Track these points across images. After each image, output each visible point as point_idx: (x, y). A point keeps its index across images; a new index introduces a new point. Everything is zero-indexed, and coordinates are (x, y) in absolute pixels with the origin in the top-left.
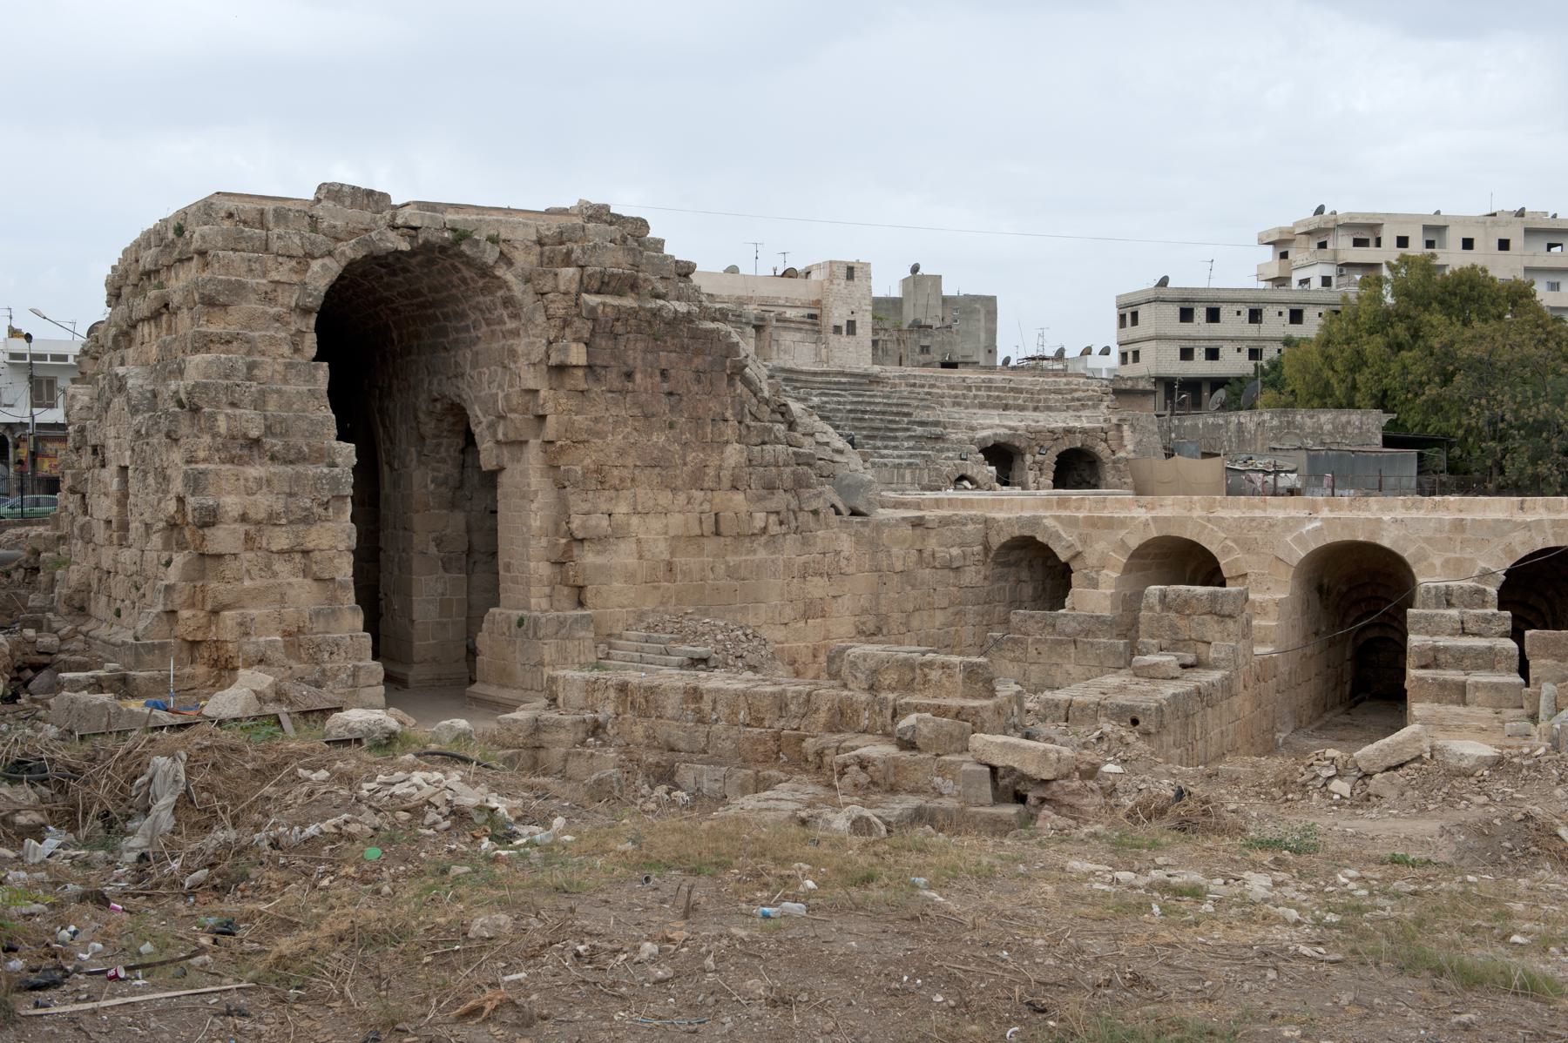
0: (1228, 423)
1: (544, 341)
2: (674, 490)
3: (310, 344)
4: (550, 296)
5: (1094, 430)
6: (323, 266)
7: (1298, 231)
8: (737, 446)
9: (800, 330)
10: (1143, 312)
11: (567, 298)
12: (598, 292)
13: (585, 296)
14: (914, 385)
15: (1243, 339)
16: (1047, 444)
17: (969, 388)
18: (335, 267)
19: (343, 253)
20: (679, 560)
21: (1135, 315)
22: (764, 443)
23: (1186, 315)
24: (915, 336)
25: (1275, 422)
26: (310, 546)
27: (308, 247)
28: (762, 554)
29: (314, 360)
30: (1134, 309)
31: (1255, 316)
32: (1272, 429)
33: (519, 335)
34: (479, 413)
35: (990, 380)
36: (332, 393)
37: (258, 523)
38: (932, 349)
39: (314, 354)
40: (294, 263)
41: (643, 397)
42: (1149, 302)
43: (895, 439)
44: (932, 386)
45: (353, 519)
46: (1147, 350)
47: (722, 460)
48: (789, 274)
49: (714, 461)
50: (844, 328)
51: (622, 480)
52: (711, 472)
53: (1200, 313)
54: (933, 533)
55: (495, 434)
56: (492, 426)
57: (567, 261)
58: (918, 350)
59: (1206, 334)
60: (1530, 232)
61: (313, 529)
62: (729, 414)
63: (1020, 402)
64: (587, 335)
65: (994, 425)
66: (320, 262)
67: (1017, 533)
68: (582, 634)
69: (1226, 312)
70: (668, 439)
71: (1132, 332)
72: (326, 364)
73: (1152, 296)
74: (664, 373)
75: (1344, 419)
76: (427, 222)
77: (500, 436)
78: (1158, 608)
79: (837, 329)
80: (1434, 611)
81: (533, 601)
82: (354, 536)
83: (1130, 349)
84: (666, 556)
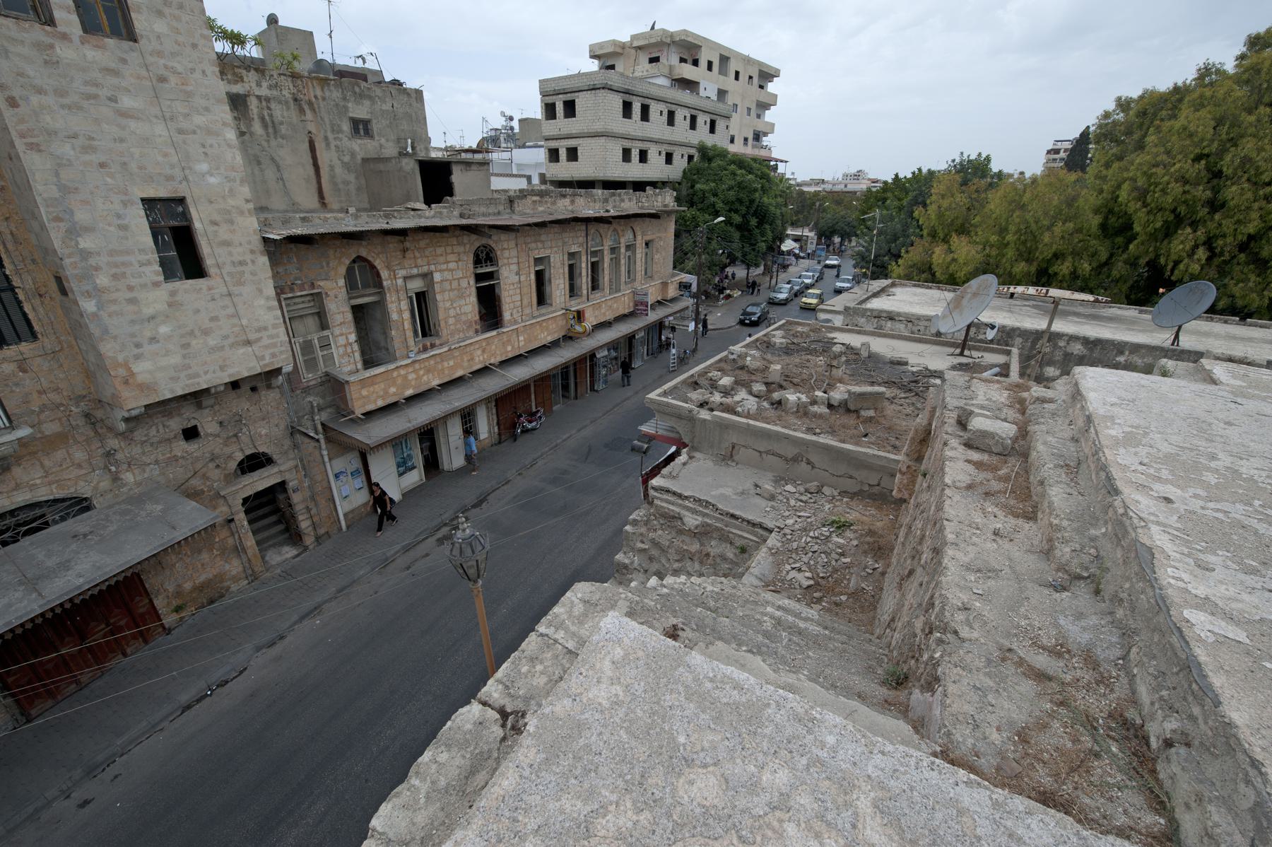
7: (636, 44)
10: (581, 102)
23: (627, 109)
24: (336, 94)
38: (375, 127)
42: (594, 89)
46: (584, 147)
58: (346, 127)
59: (639, 134)
71: (562, 124)
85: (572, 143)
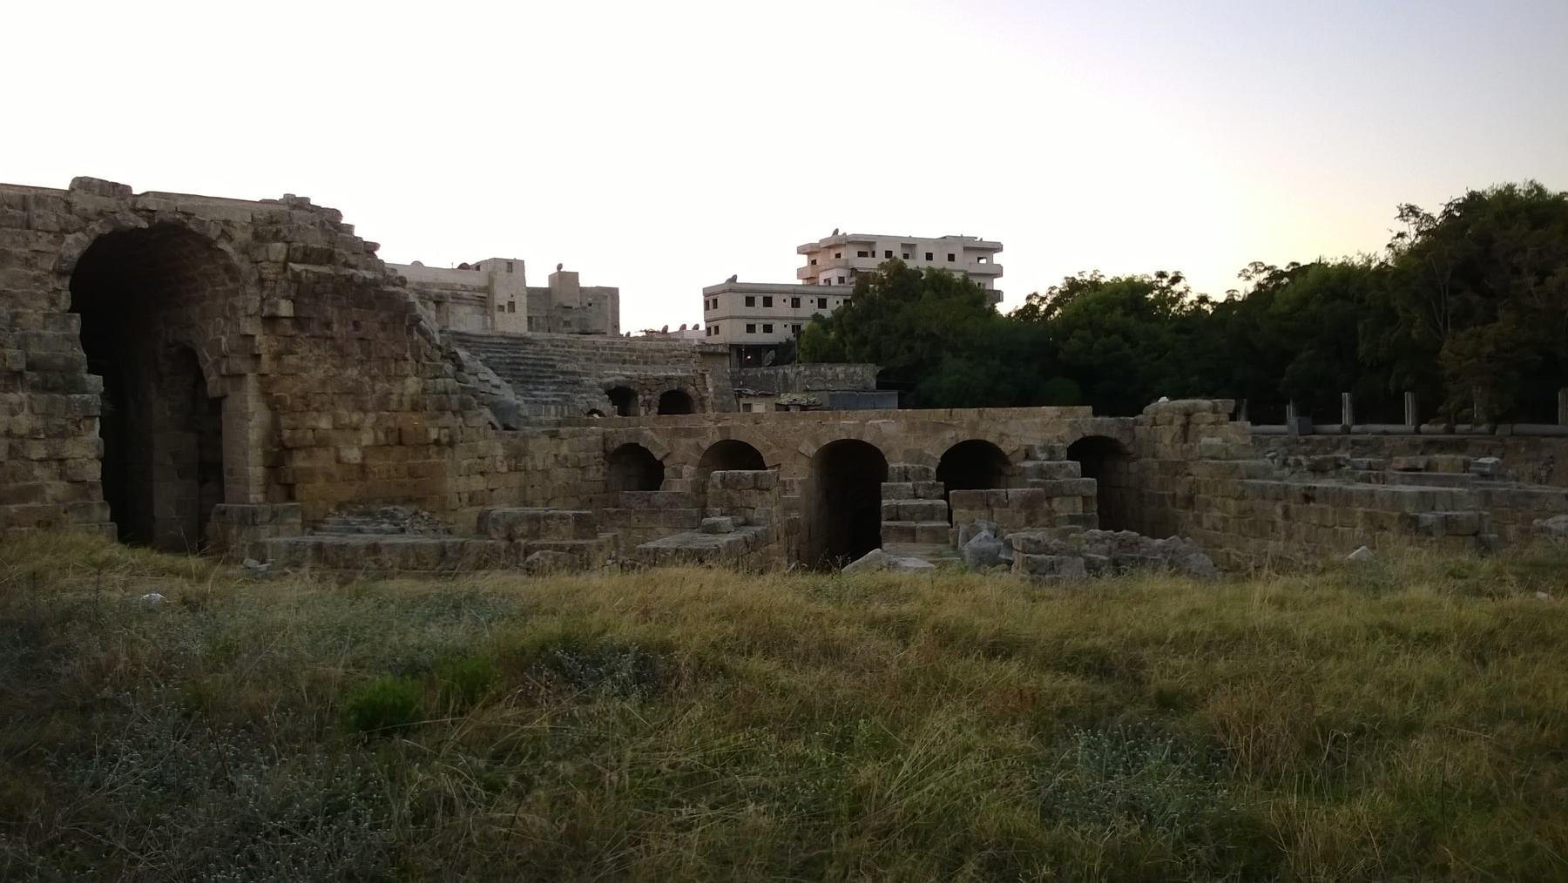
0: (777, 373)
1: (259, 298)
2: (365, 412)
3: (65, 300)
4: (264, 264)
5: (687, 377)
6: (77, 240)
7: (822, 246)
8: (415, 379)
9: (470, 304)
10: (720, 298)
11: (276, 266)
12: (302, 262)
13: (291, 264)
14: (557, 346)
15: (787, 318)
16: (653, 388)
17: (598, 349)
18: (85, 239)
19: (93, 230)
20: (369, 462)
21: (715, 301)
22: (437, 377)
23: (750, 302)
25: (807, 373)
26: (65, 455)
27: (63, 225)
28: (435, 459)
29: (69, 311)
30: (715, 297)
31: (796, 303)
32: (805, 377)
33: (238, 294)
34: (207, 355)
35: (613, 343)
36: (83, 336)
37: (21, 437)
39: (68, 307)
40: (51, 236)
41: (340, 342)
42: (724, 292)
43: (543, 383)
44: (570, 347)
45: (101, 434)
46: (723, 325)
47: (404, 389)
48: (464, 267)
49: (397, 389)
50: (506, 307)
51: (323, 404)
52: (395, 397)
53: (759, 300)
54: (565, 442)
55: (219, 370)
56: (217, 363)
57: (276, 236)
58: (562, 324)
59: (762, 315)
60: (966, 249)
61: (67, 441)
62: (408, 355)
63: (634, 358)
64: (293, 294)
65: (616, 374)
66: (73, 236)
67: (625, 441)
68: (291, 520)
69: (776, 300)
70: (360, 373)
71: (714, 313)
72: (78, 315)
73: (726, 288)
74: (356, 325)
75: (852, 370)
76: (162, 207)
77: (224, 371)
78: (720, 486)
79: (501, 308)
80: (896, 484)
81: (252, 496)
82: (102, 447)
83: (713, 324)
84: (359, 461)
85: (716, 323)
